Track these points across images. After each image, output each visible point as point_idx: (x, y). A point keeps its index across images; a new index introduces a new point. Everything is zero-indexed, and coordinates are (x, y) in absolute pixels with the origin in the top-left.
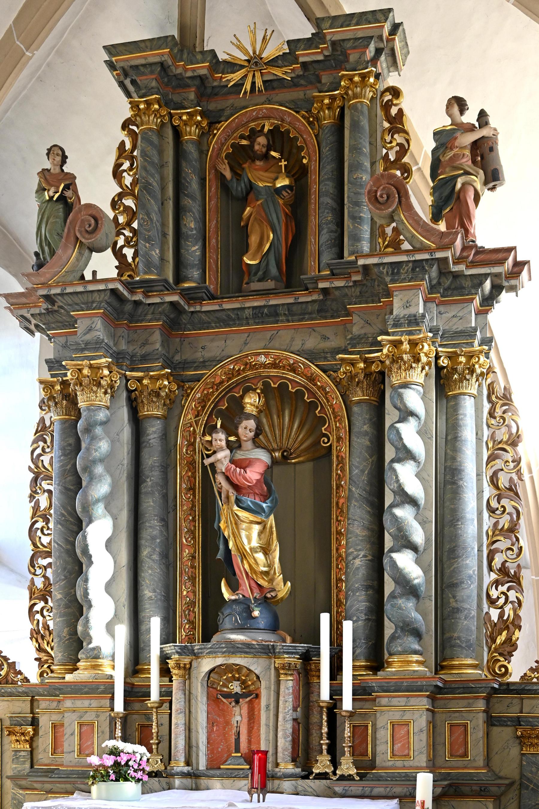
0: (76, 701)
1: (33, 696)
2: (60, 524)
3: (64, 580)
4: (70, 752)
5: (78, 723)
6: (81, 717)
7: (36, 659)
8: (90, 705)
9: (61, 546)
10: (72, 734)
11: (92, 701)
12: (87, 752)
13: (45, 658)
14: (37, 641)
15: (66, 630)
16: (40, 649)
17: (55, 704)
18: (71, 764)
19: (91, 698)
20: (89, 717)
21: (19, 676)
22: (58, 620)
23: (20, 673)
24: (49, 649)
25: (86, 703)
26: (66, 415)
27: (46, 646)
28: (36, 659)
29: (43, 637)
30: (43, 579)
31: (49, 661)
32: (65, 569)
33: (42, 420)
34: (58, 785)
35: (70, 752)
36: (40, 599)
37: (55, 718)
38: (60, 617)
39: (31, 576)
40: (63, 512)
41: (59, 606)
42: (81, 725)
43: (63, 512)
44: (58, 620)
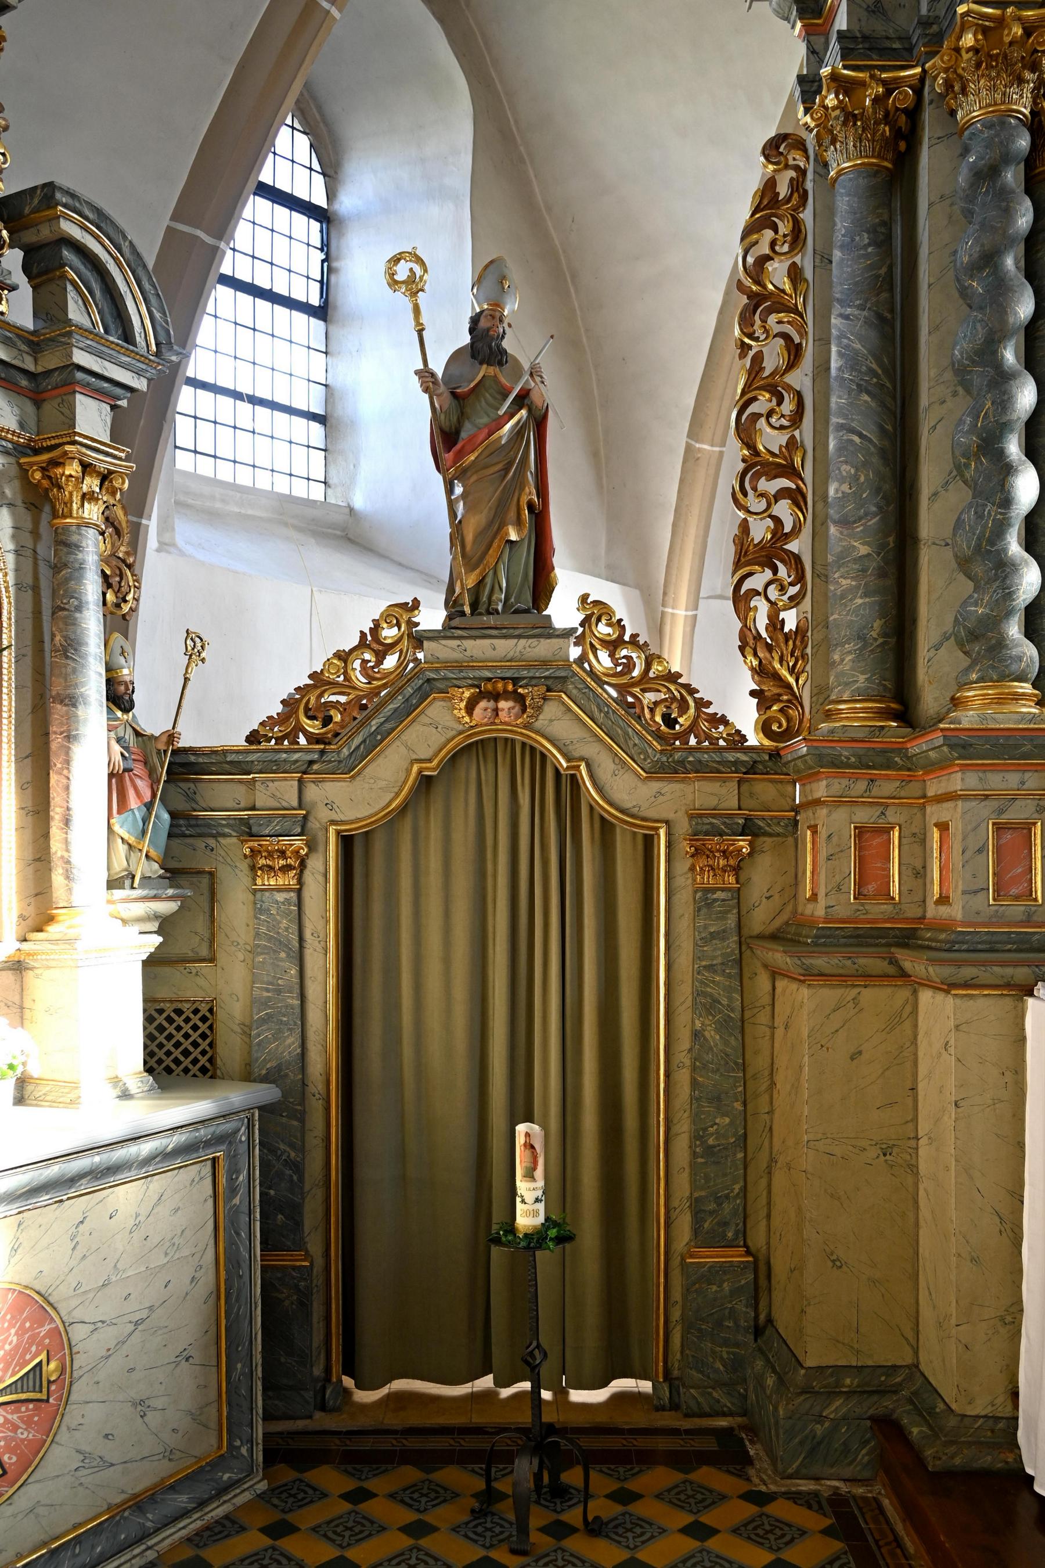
0: (989, 775)
1: (764, 765)
2: (868, 393)
3: (875, 515)
4: (976, 892)
5: (994, 824)
6: (1001, 811)
7: (753, 693)
8: (1023, 783)
9: (870, 441)
10: (979, 851)
11: (1027, 775)
12: (1014, 891)
13: (776, 691)
14: (755, 655)
15: (877, 624)
16: (761, 672)
17: (861, 786)
18: (980, 920)
19: (1023, 769)
20: (1017, 813)
21: (721, 728)
22: (859, 601)
23: (724, 720)
24: (784, 673)
25: (1013, 779)
26: (879, 157)
27: (777, 666)
28: (753, 693)
29: (769, 648)
30: (769, 522)
31: (785, 698)
32: (878, 490)
33: (769, 185)
34: (995, 968)
35: (976, 892)
36: (763, 565)
37: (864, 816)
38: (866, 595)
39: (742, 515)
40: (874, 366)
41: (864, 570)
42: (999, 828)
43: (874, 366)
44: (859, 601)
